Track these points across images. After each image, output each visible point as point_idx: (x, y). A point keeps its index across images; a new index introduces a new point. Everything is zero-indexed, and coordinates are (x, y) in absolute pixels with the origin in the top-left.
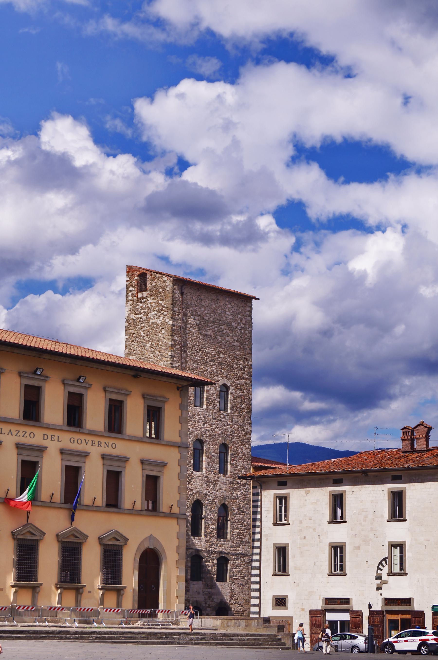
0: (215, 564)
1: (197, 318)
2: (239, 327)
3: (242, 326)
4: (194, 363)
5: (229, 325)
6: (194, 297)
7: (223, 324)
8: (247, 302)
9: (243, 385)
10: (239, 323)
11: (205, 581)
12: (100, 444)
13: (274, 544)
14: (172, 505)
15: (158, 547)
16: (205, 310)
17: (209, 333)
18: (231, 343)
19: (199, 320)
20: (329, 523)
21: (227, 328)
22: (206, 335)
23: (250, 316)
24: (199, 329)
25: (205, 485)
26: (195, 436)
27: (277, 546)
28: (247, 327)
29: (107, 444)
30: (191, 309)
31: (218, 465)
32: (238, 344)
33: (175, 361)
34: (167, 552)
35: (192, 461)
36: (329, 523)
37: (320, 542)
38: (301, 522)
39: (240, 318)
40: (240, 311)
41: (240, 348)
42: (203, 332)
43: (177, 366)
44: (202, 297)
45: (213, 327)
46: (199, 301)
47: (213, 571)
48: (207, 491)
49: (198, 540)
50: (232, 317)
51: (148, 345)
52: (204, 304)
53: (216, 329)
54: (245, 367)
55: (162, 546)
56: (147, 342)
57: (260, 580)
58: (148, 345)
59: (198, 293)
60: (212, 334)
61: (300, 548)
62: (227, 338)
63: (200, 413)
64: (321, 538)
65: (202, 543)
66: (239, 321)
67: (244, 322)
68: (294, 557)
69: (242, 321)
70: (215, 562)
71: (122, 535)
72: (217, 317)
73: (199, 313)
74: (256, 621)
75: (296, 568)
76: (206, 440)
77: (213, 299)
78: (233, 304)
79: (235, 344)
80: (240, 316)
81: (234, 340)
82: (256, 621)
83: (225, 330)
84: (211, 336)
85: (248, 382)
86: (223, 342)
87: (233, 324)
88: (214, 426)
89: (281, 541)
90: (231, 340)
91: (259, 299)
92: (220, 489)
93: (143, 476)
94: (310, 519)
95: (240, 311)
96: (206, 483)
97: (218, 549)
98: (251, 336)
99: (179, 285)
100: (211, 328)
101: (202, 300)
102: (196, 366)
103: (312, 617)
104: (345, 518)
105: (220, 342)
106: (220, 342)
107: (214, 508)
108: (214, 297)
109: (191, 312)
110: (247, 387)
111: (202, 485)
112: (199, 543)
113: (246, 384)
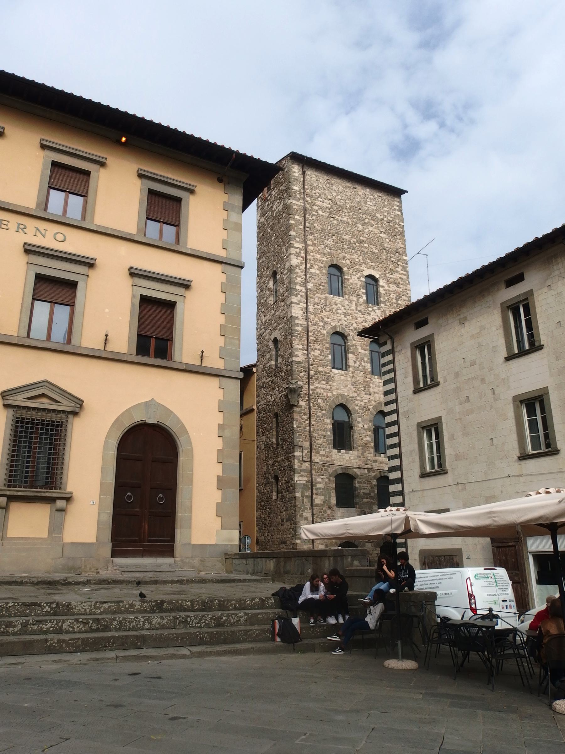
0: (375, 485)
1: (326, 201)
2: (385, 219)
3: (391, 219)
4: (325, 247)
5: (374, 217)
6: (320, 180)
7: (364, 214)
8: (394, 196)
9: (397, 279)
10: (385, 216)
11: (360, 508)
12: (21, 228)
13: (419, 424)
14: (202, 352)
15: (168, 423)
16: (338, 195)
17: (345, 219)
18: (376, 234)
19: (329, 204)
20: (508, 359)
21: (370, 218)
22: (341, 221)
23: (401, 211)
24: (331, 213)
25: (352, 387)
26: (331, 328)
27: (424, 425)
28: (397, 221)
29: (43, 232)
30: (318, 191)
31: (369, 365)
32: (387, 237)
33: (297, 242)
34: (193, 434)
35: (330, 357)
36: (508, 359)
37: (495, 400)
38: (457, 375)
39: (386, 211)
40: (386, 203)
41: (390, 241)
42: (337, 217)
43: (301, 247)
44: (333, 182)
45: (351, 214)
46: (328, 185)
47: (372, 494)
48: (356, 394)
49: (345, 455)
50: (375, 208)
51: (273, 238)
52: (336, 189)
53: (354, 216)
54: (398, 261)
55: (179, 421)
56: (271, 236)
57: (403, 488)
58: (273, 238)
59: (326, 177)
60: (349, 220)
61: (461, 419)
62: (371, 228)
63: (337, 302)
64: (496, 392)
65: (352, 458)
66: (386, 214)
67: (392, 216)
68: (452, 437)
69: (389, 214)
70: (375, 482)
71: (65, 391)
72: (356, 205)
73: (329, 197)
74: (332, 558)
75: (458, 457)
76: (349, 334)
77: (348, 187)
78: (376, 196)
79: (383, 235)
80: (385, 209)
81: (381, 232)
82: (332, 558)
83: (367, 220)
84: (348, 223)
85: (405, 277)
86: (366, 231)
87: (378, 215)
88: (360, 320)
89: (427, 415)
90: (376, 231)
91: (407, 192)
92: (375, 393)
93: (133, 296)
94: (473, 364)
95: (386, 203)
96: (352, 385)
97: (376, 466)
98: (403, 231)
99: (298, 165)
100: (348, 214)
101: (332, 185)
102: (329, 251)
103: (497, 547)
104: (540, 341)
105: (361, 231)
106: (361, 231)
107: (368, 416)
108: (349, 184)
109: (317, 194)
110: (402, 283)
111: (347, 386)
112: (348, 458)
113: (401, 278)
